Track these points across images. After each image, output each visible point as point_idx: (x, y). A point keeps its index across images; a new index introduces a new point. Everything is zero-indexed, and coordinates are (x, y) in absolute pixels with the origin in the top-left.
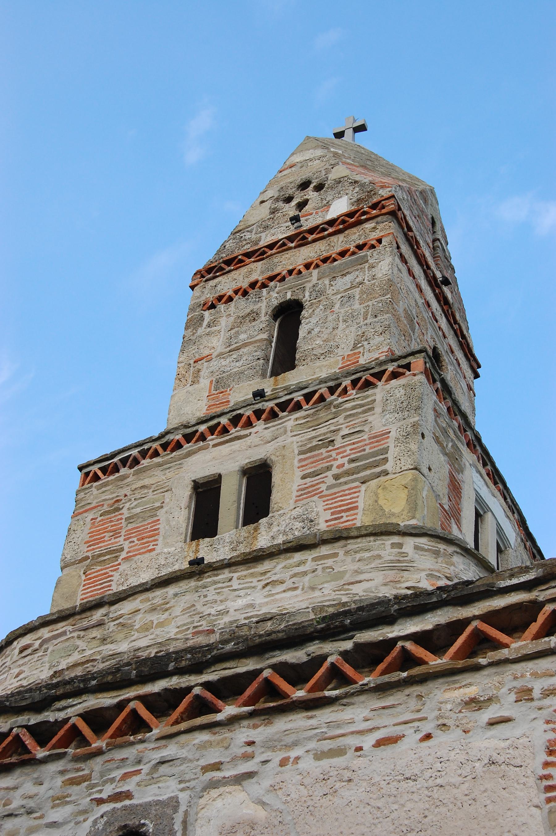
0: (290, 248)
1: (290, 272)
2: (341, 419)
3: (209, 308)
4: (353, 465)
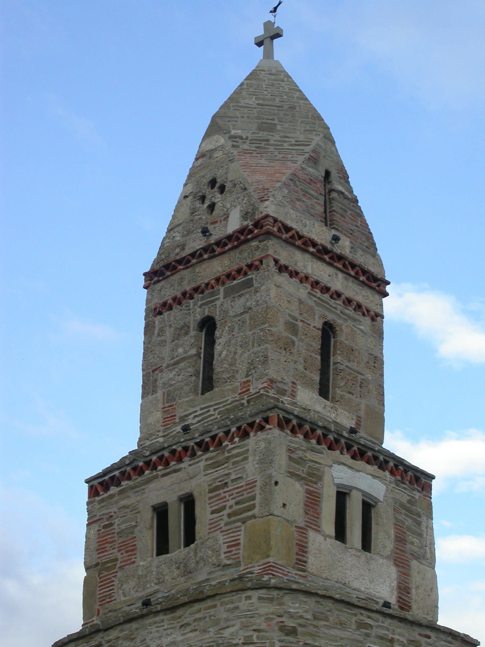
2: (230, 465)
4: (238, 507)
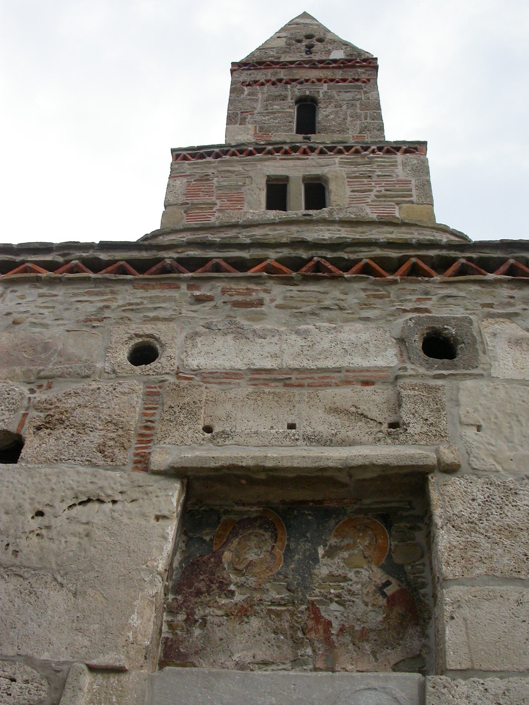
0: (305, 68)
1: (307, 81)
3: (247, 86)
